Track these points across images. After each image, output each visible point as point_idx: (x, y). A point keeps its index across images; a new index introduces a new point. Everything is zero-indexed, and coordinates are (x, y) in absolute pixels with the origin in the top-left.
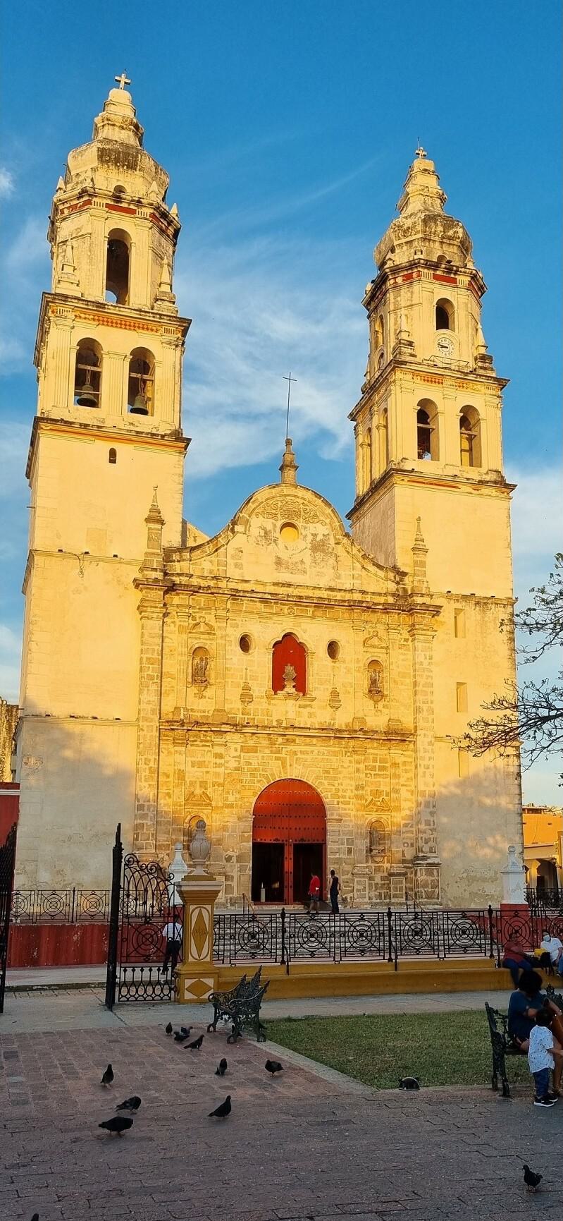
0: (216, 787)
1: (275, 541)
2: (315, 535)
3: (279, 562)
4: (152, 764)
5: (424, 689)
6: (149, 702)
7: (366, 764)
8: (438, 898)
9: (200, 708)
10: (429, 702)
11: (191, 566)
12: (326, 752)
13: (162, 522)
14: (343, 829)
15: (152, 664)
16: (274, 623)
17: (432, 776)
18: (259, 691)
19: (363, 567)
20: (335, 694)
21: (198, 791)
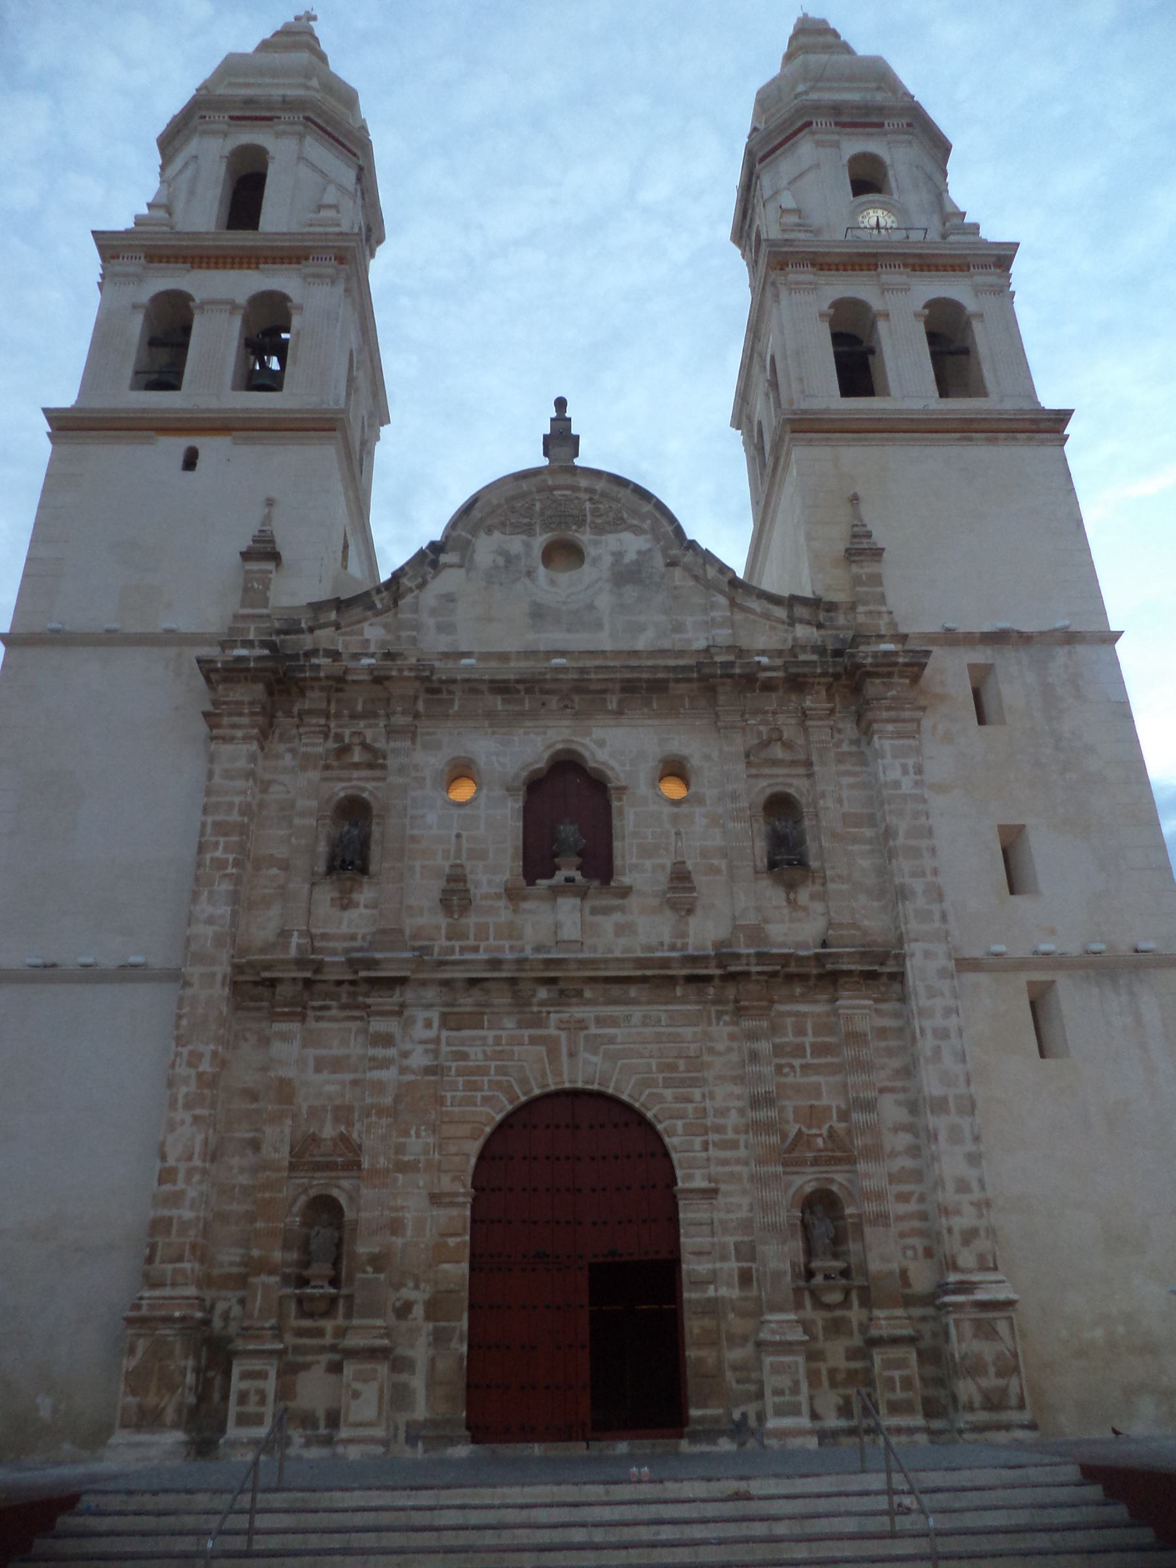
0: (374, 1118)
1: (529, 573)
2: (618, 555)
3: (539, 614)
5: (913, 842)
6: (210, 921)
7: (777, 1040)
8: (1021, 1406)
9: (344, 929)
10: (928, 872)
11: (341, 639)
12: (664, 1017)
13: (274, 557)
14: (722, 1215)
15: (226, 834)
16: (526, 733)
17: (962, 1058)
18: (490, 882)
19: (733, 604)
20: (681, 878)
21: (328, 1131)
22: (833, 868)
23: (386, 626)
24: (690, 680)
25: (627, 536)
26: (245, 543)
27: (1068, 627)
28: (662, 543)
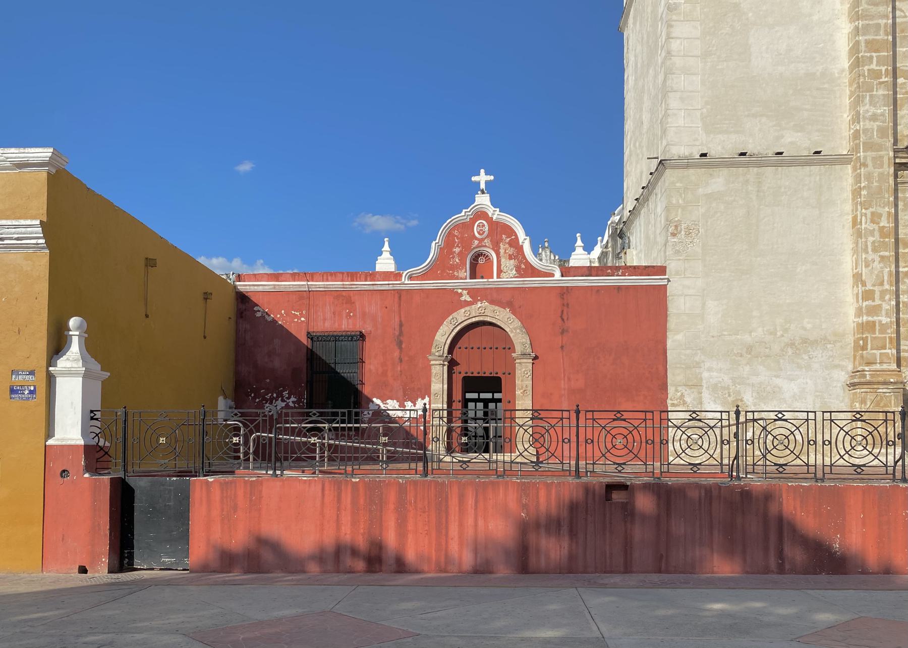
4: (883, 223)
6: (874, 118)
15: (877, 51)
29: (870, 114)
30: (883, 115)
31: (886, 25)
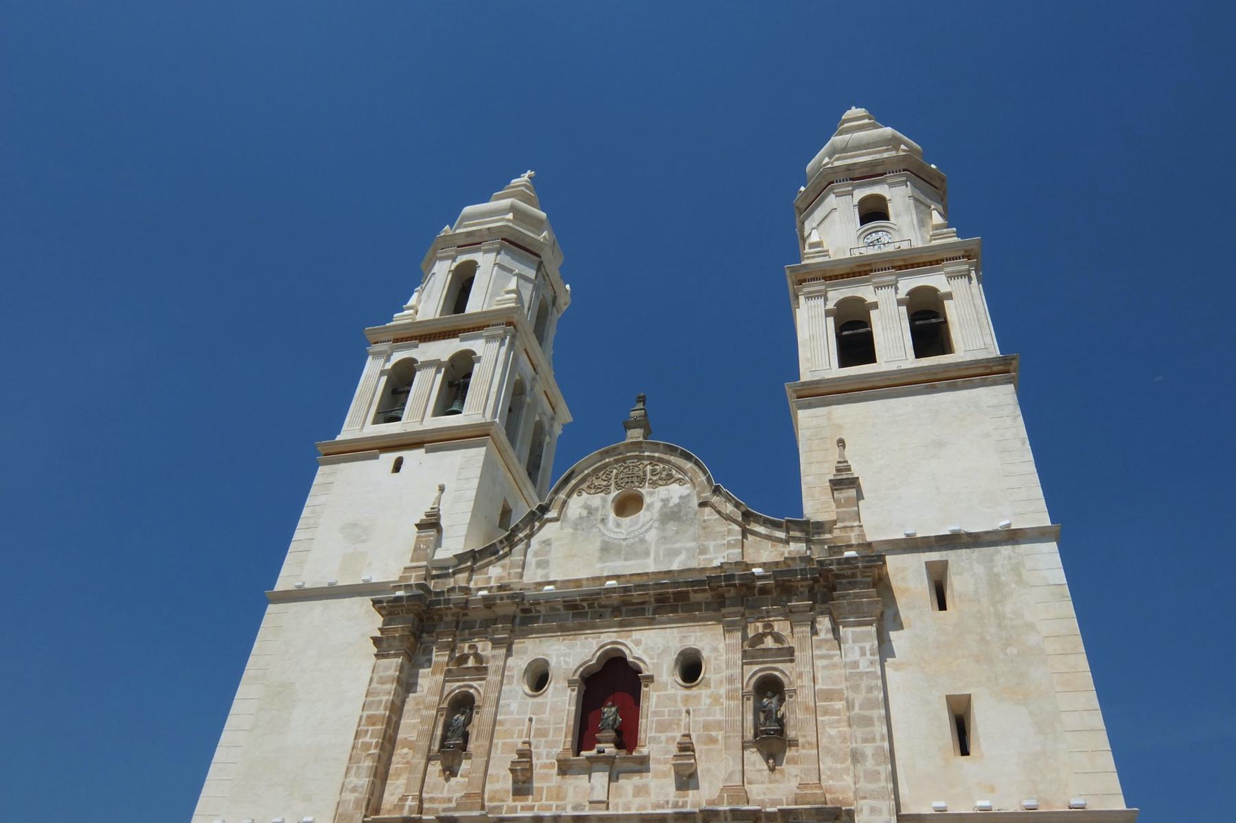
1: (603, 520)
2: (665, 501)
6: (354, 789)
9: (445, 794)
15: (374, 724)
16: (586, 638)
18: (548, 756)
20: (686, 748)
22: (804, 736)
23: (503, 567)
24: (705, 591)
25: (675, 486)
26: (420, 517)
27: (1009, 525)
28: (697, 489)
29: (352, 785)
30: (362, 786)
31: (387, 701)
